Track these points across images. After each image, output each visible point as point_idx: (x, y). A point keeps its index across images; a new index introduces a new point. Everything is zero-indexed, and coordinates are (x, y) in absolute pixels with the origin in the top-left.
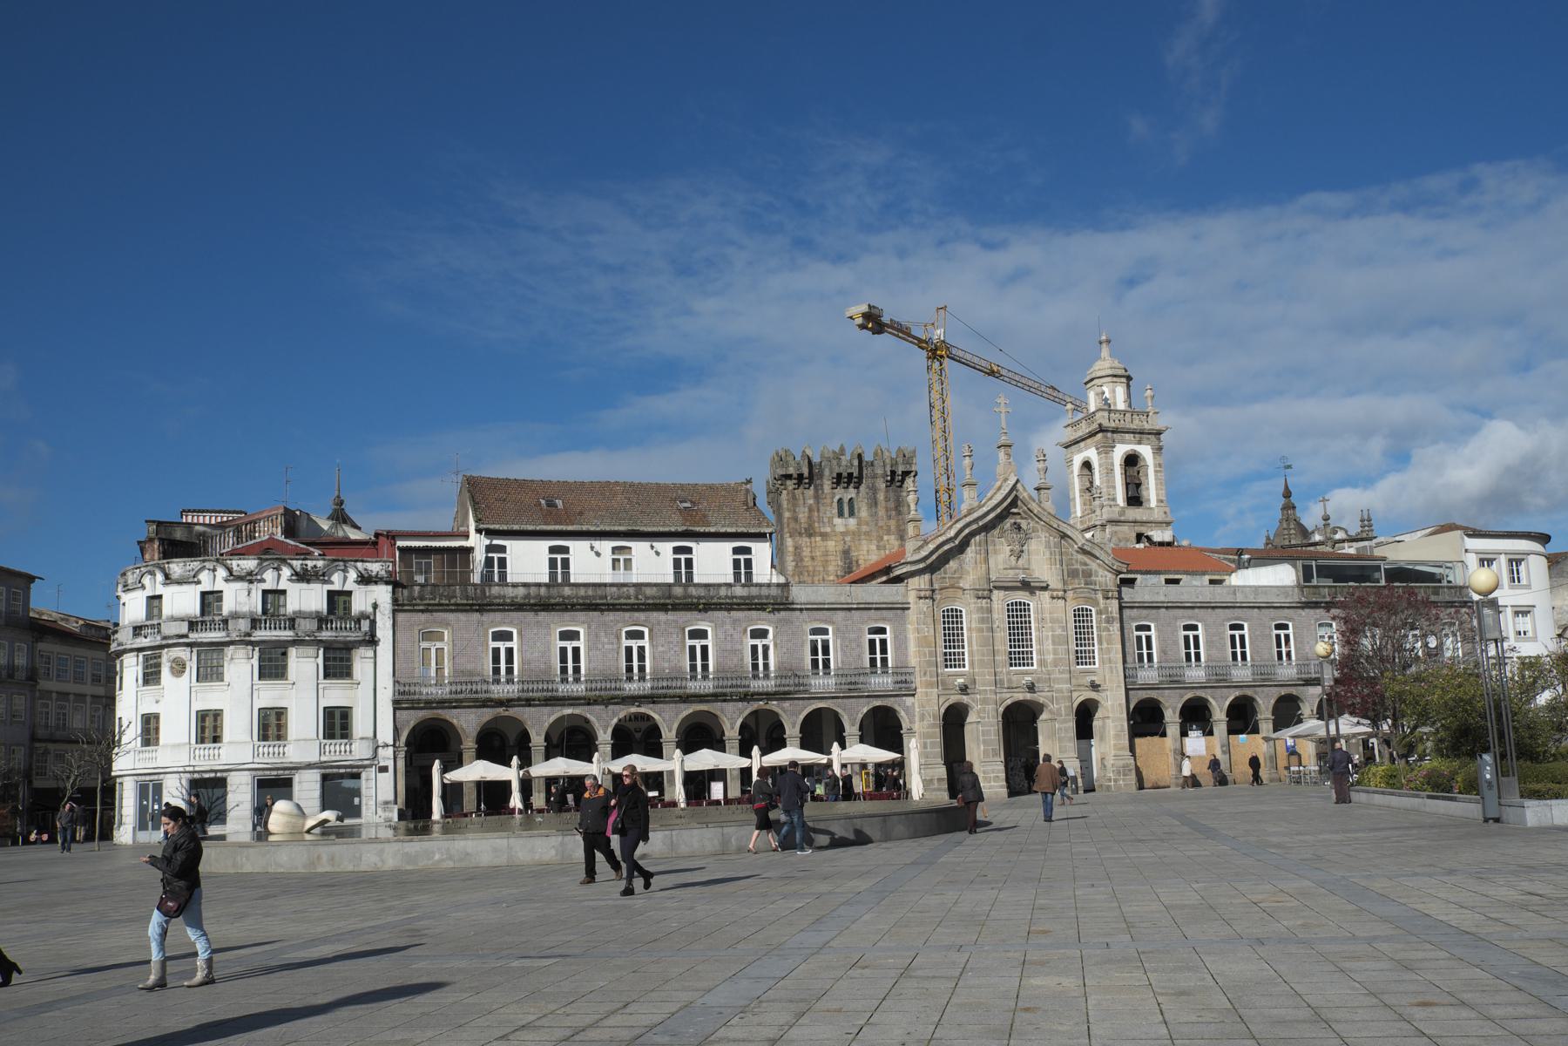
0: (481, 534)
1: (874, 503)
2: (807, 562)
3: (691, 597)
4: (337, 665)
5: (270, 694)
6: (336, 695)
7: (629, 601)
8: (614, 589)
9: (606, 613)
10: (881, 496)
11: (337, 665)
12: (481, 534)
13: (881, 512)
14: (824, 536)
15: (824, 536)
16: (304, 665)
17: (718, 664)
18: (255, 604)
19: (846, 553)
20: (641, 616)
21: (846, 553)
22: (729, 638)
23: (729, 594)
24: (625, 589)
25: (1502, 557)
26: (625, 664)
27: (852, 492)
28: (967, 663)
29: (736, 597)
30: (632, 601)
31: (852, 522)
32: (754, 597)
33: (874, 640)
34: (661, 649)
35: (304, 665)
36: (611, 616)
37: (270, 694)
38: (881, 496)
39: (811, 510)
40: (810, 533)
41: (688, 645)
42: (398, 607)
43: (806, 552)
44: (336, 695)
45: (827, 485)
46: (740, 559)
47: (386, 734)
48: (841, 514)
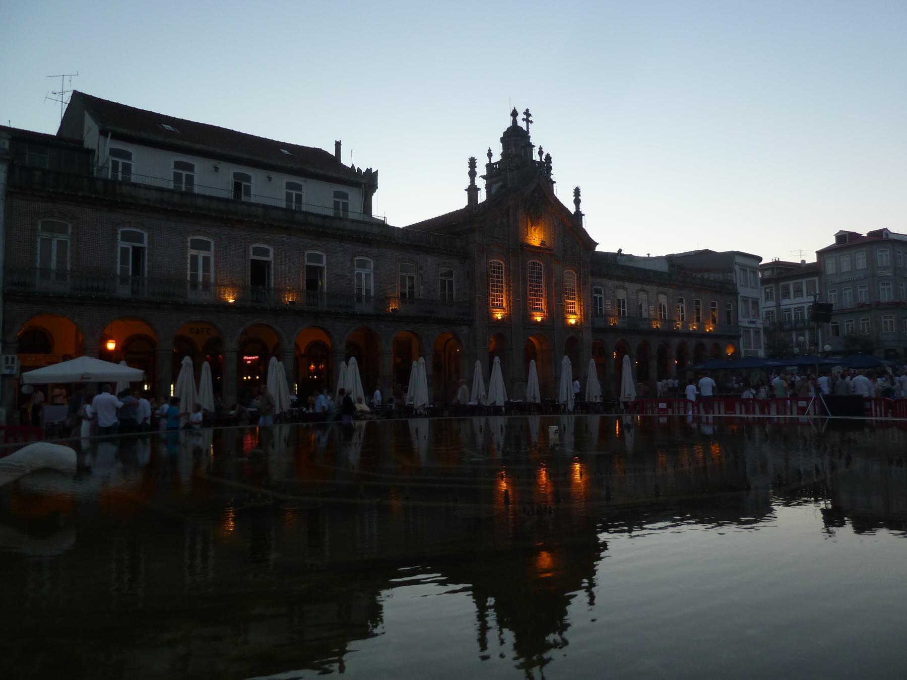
0: (106, 136)
12: (106, 136)
25: (748, 268)
33: (445, 281)
46: (339, 202)
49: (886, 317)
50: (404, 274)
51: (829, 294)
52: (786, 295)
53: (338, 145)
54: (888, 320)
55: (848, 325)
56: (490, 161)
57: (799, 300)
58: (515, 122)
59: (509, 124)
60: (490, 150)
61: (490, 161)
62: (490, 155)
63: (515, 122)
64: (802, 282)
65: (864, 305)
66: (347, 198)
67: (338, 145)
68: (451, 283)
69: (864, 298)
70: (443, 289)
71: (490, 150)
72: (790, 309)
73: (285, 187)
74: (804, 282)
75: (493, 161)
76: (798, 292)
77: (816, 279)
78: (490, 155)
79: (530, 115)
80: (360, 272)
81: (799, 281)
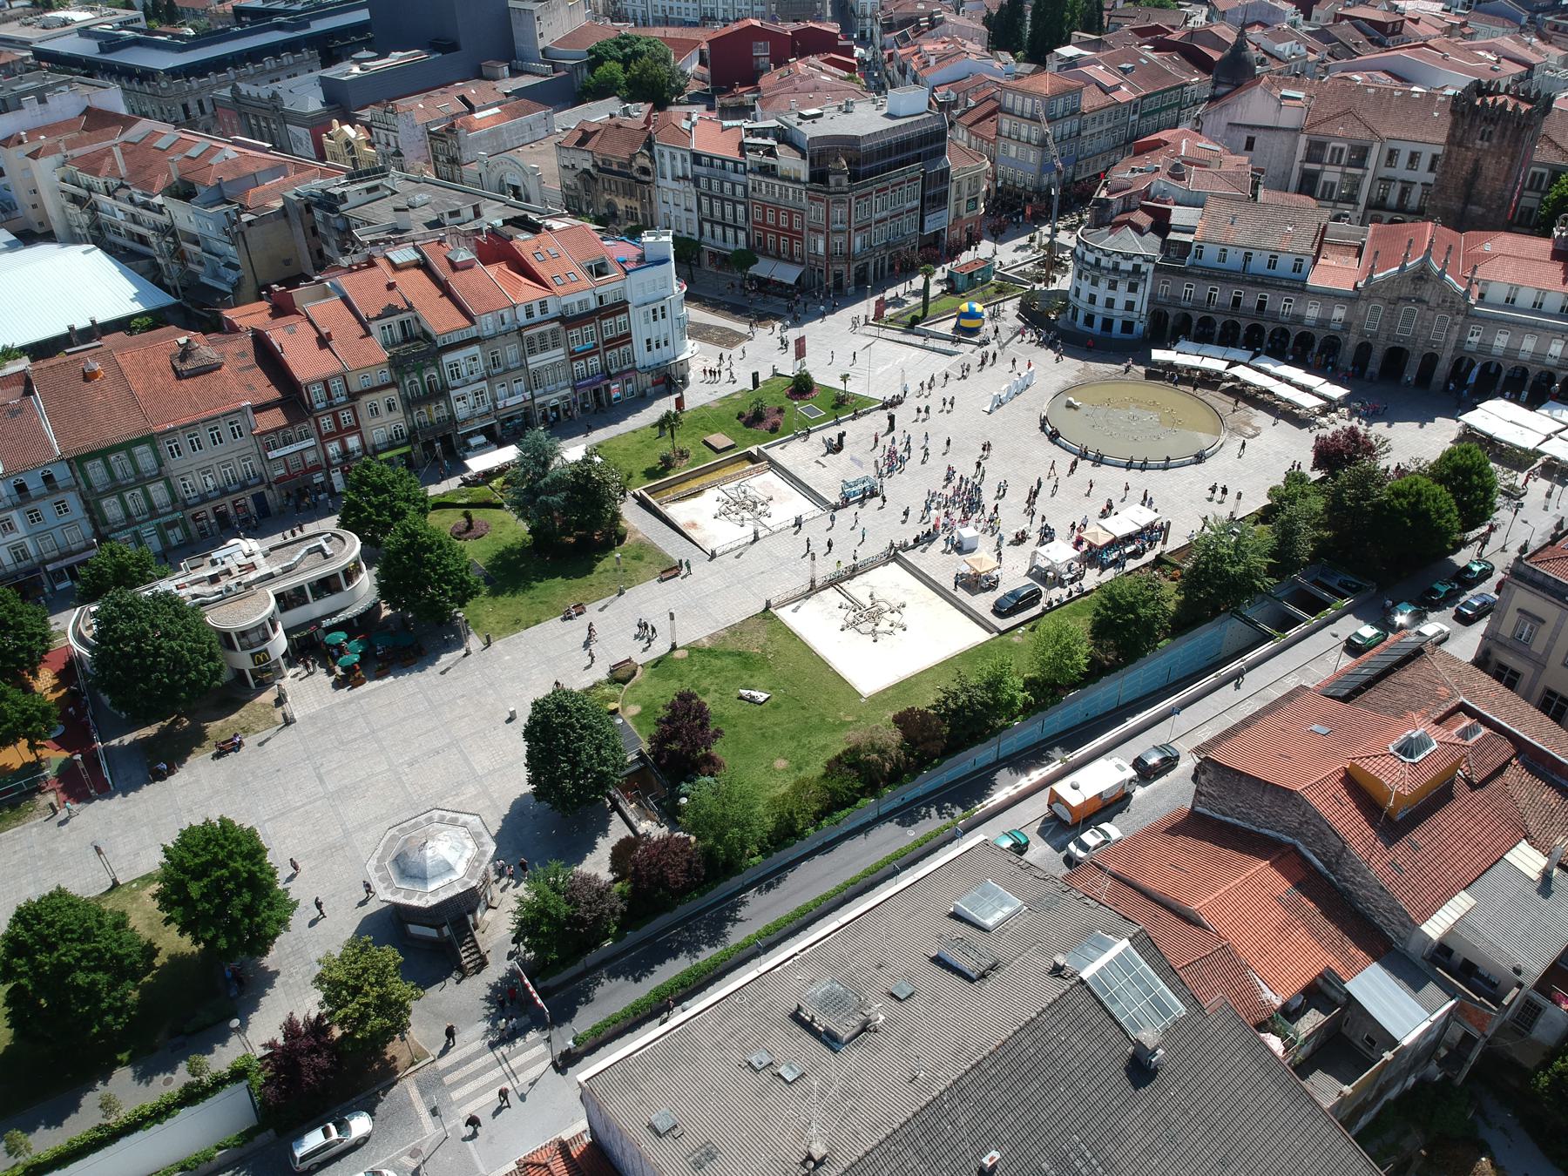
1: (1503, 135)
2: (1453, 161)
4: (1133, 288)
5: (1111, 294)
6: (1131, 297)
10: (1508, 133)
11: (1133, 288)
13: (1505, 144)
14: (1468, 149)
15: (1468, 149)
16: (1123, 287)
18: (1110, 265)
19: (1477, 161)
21: (1477, 161)
27: (1492, 128)
31: (1487, 144)
35: (1123, 287)
37: (1111, 294)
38: (1508, 133)
39: (1464, 132)
40: (1460, 145)
42: (1155, 271)
43: (1454, 155)
44: (1131, 297)
45: (1478, 122)
47: (1144, 311)
48: (1482, 139)
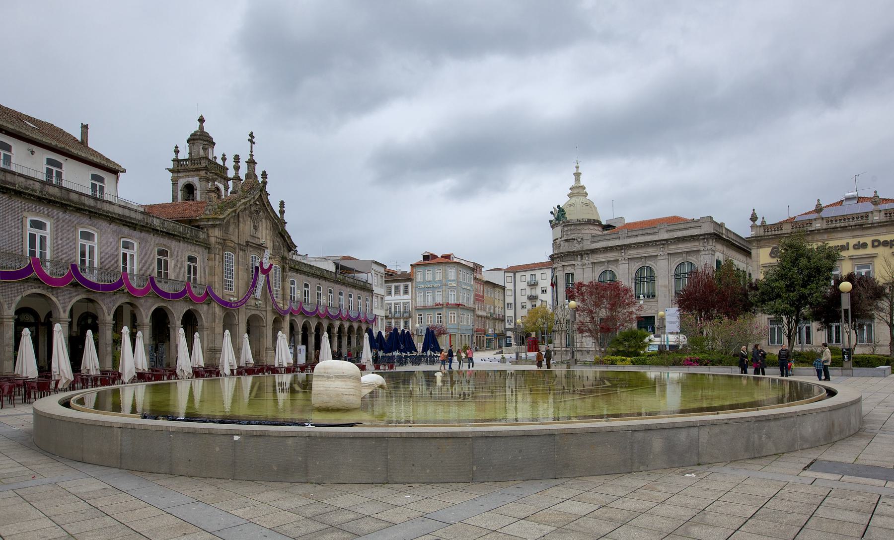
3: (84, 205)
7: (34, 193)
8: (22, 179)
9: (14, 198)
17: (101, 262)
20: (45, 209)
22: (109, 244)
23: (111, 210)
24: (31, 182)
26: (28, 249)
28: (233, 288)
29: (115, 213)
30: (38, 194)
32: (131, 218)
34: (60, 242)
36: (17, 203)
41: (80, 243)
49: (451, 313)
50: (160, 257)
51: (417, 295)
52: (389, 293)
53: (85, 128)
54: (453, 315)
55: (428, 317)
56: (177, 157)
57: (398, 297)
58: (201, 128)
59: (195, 127)
60: (177, 147)
61: (177, 157)
62: (177, 152)
63: (201, 128)
64: (400, 285)
65: (439, 304)
66: (103, 182)
67: (85, 128)
68: (195, 268)
69: (439, 300)
70: (189, 272)
71: (177, 147)
72: (391, 303)
73: (46, 164)
74: (402, 285)
75: (180, 157)
76: (397, 292)
77: (410, 283)
78: (177, 152)
79: (254, 137)
80: (126, 252)
81: (399, 284)
